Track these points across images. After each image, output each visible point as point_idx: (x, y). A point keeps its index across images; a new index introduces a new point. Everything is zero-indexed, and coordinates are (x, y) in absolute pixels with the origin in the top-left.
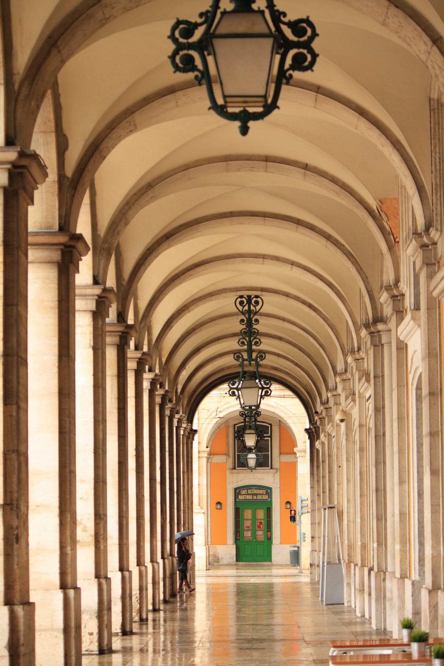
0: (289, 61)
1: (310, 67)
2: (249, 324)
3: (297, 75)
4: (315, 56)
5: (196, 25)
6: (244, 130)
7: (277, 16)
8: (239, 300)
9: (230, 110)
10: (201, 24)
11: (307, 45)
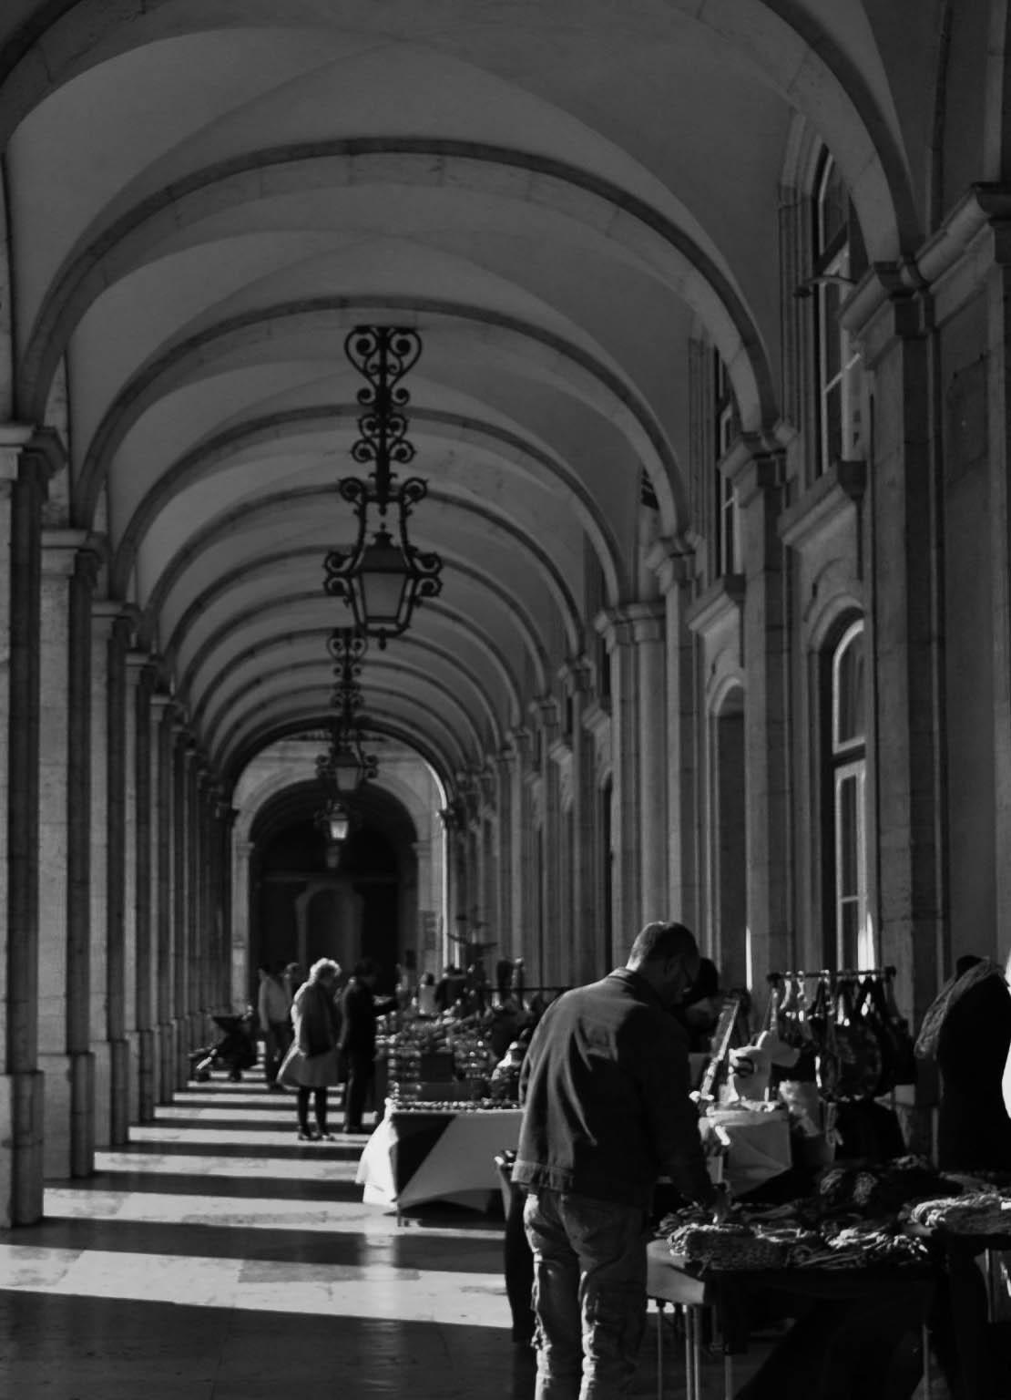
0: (419, 590)
1: (436, 594)
2: (347, 675)
3: (426, 599)
4: (440, 585)
5: (345, 558)
6: (383, 646)
7: (411, 551)
8: (333, 641)
9: (374, 626)
10: (349, 557)
11: (434, 575)
